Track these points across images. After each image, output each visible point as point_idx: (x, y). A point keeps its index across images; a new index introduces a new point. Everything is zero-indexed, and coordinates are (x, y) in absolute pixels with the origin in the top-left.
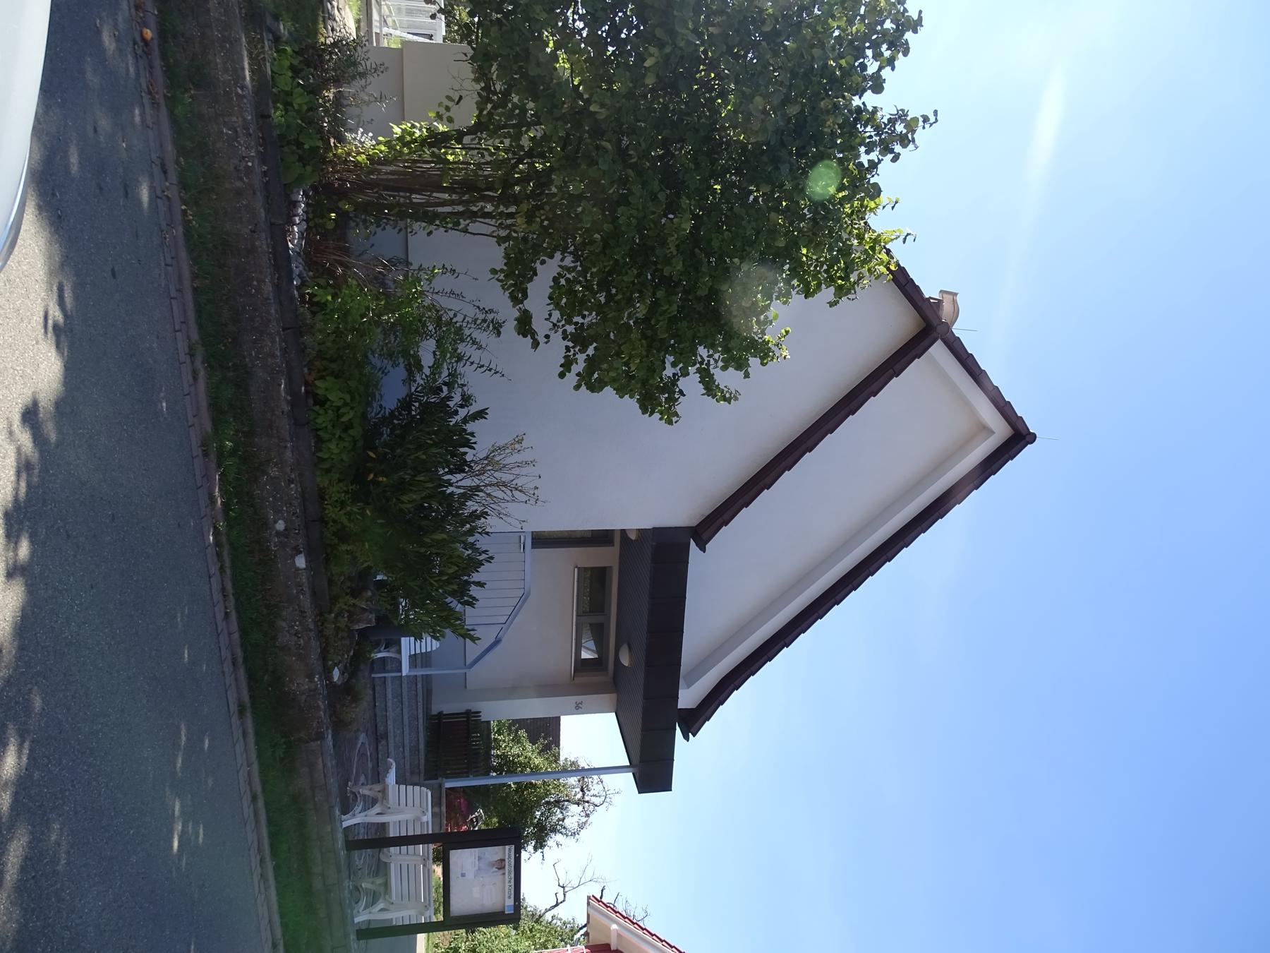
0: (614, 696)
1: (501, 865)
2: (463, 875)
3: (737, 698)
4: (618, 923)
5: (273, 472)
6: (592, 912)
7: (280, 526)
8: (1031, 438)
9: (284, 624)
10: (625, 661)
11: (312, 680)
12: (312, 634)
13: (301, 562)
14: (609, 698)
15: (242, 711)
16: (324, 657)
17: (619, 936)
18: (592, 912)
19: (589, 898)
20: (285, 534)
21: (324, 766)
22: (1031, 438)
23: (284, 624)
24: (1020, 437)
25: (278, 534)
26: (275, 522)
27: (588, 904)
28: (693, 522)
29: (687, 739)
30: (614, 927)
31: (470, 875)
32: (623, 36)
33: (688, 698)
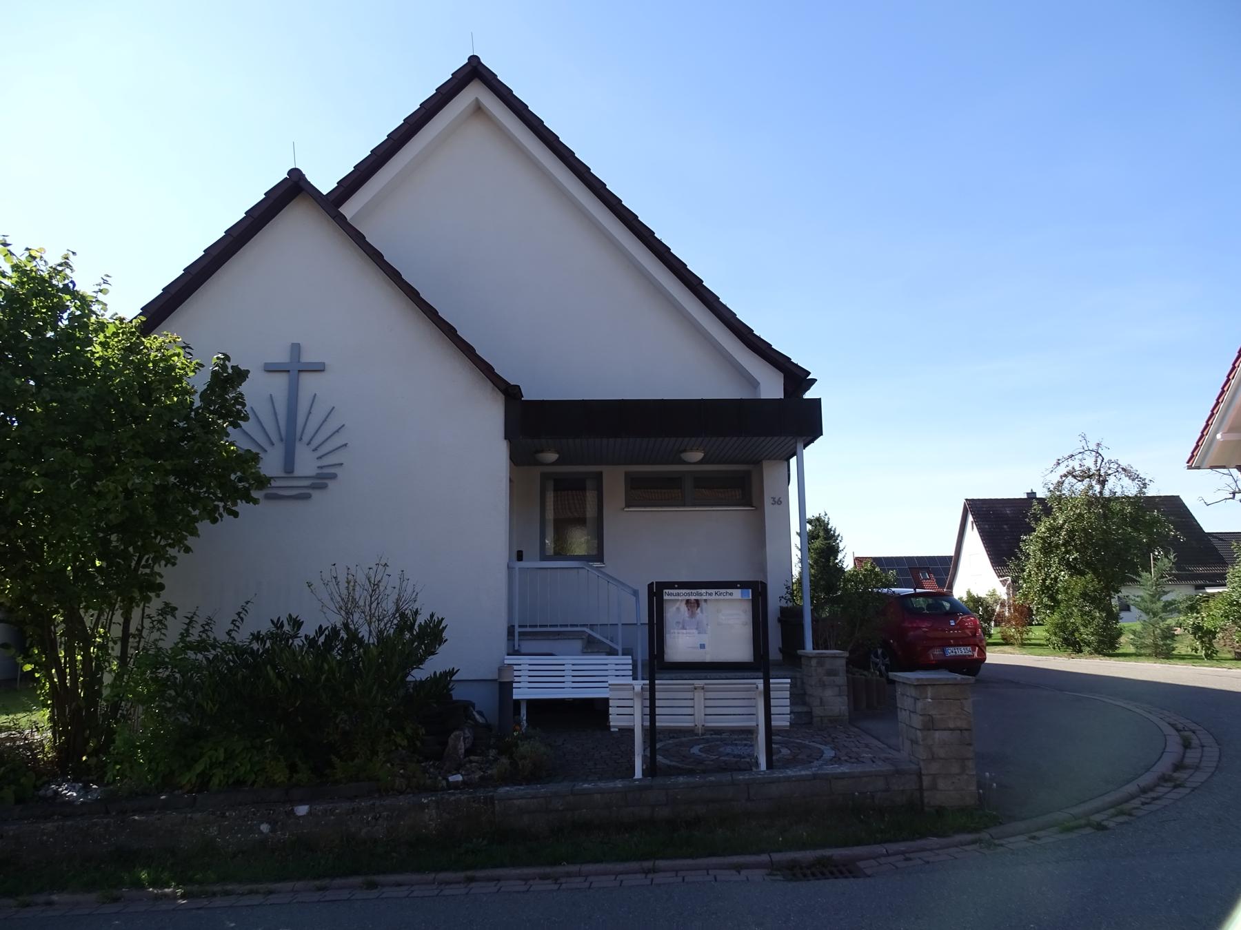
0: (765, 464)
1: (694, 605)
2: (702, 646)
3: (761, 330)
4: (1216, 433)
5: (214, 831)
6: (1208, 462)
7: (265, 828)
8: (474, 60)
9: (364, 831)
10: (699, 456)
11: (427, 806)
12: (378, 803)
13: (302, 810)
14: (770, 472)
15: (372, 886)
16: (433, 790)
17: (1231, 430)
18: (1208, 462)
19: (1190, 468)
20: (273, 824)
21: (522, 798)
22: (474, 60)
23: (364, 831)
24: (474, 72)
25: (273, 830)
26: (262, 833)
27: (1198, 468)
28: (500, 398)
29: (814, 381)
30: (1219, 436)
31: (704, 639)
32: (233, 477)
33: (772, 387)
